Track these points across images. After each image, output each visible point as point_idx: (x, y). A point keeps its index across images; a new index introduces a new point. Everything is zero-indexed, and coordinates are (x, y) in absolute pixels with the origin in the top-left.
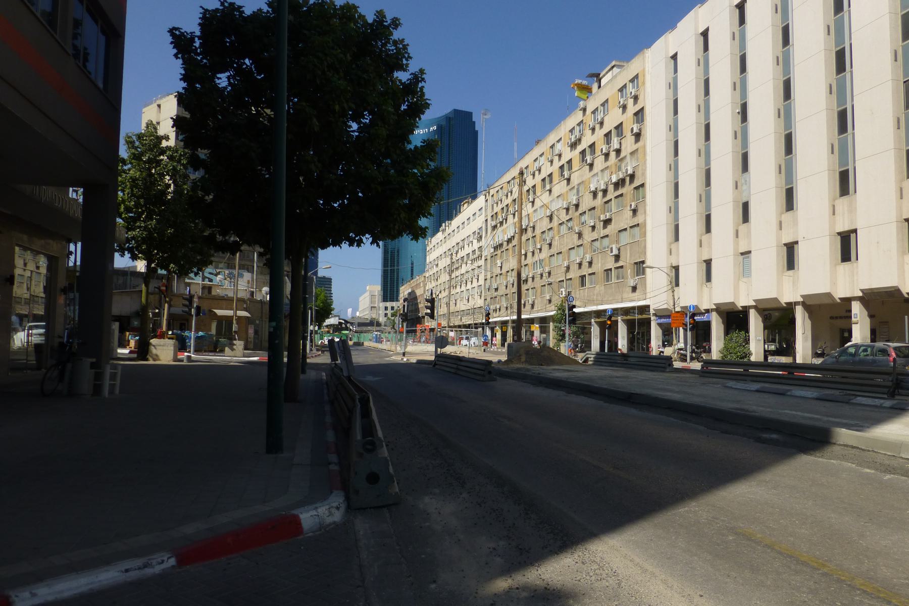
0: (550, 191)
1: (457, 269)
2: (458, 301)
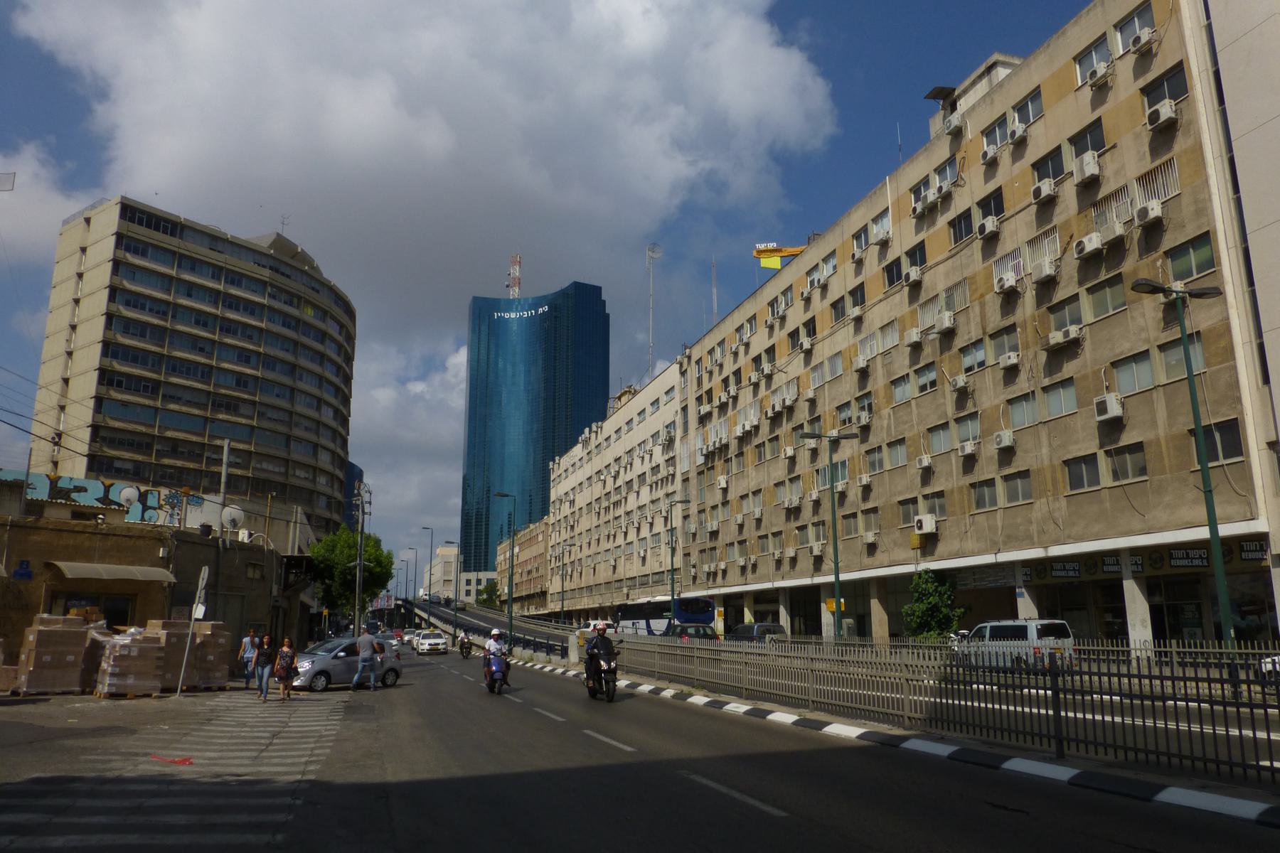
0: (859, 321)
1: (617, 504)
2: (621, 562)
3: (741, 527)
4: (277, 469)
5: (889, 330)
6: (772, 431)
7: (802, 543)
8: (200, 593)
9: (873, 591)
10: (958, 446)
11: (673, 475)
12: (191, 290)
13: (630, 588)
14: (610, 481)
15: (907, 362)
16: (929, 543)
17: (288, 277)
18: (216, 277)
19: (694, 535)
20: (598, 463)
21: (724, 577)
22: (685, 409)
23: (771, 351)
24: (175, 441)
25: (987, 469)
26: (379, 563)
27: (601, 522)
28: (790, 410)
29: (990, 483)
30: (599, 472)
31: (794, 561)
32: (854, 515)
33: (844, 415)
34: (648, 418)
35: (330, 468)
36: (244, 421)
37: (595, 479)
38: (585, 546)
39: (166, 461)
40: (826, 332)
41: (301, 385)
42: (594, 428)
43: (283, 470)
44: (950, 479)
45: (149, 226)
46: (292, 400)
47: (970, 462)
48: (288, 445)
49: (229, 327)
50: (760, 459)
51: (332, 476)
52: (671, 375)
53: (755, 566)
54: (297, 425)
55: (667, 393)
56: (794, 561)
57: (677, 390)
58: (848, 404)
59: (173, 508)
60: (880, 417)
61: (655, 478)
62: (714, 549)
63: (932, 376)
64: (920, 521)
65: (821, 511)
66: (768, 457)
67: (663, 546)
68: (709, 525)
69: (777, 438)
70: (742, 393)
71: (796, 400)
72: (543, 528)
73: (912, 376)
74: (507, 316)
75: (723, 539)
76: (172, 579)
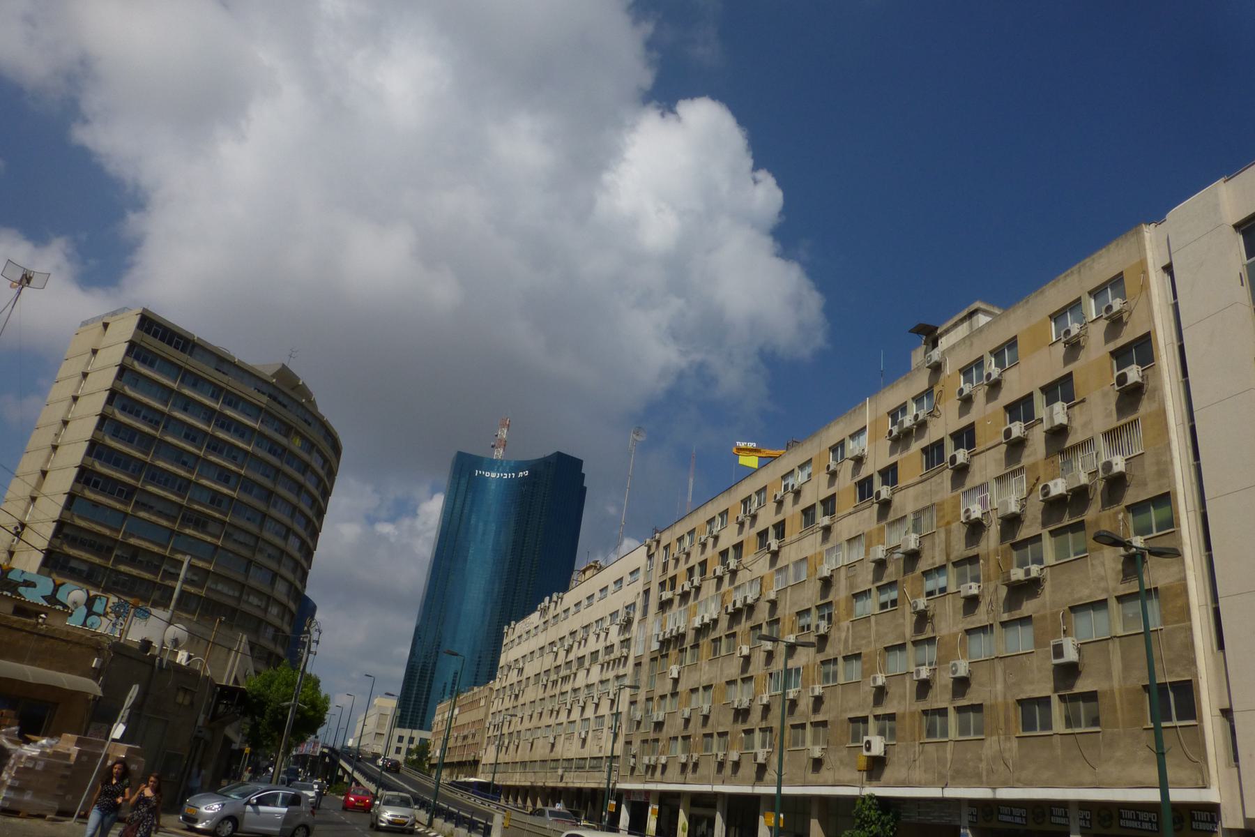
0: (827, 530)
3: (687, 721)
4: (231, 593)
5: (856, 544)
6: (730, 627)
7: (747, 748)
8: (124, 713)
9: (815, 809)
10: (913, 669)
11: (626, 658)
12: (188, 405)
13: (566, 769)
14: (562, 654)
15: (870, 577)
16: (876, 767)
17: (285, 406)
18: (215, 396)
19: (639, 723)
20: (553, 634)
21: (663, 772)
22: (647, 592)
23: (738, 547)
24: (137, 549)
25: (940, 698)
26: (314, 706)
27: (546, 695)
28: (751, 608)
29: (943, 712)
30: (552, 644)
31: (736, 765)
32: (803, 726)
33: (803, 622)
34: (609, 596)
35: (284, 599)
36: (209, 539)
37: (547, 650)
38: (526, 718)
39: (123, 568)
40: (795, 537)
41: (274, 512)
42: (555, 598)
43: (237, 594)
44: (902, 703)
45: (162, 339)
46: (261, 526)
47: (924, 687)
48: (247, 571)
49: (216, 446)
50: (715, 654)
51: (284, 607)
52: (639, 557)
53: (696, 765)
54: (261, 551)
55: (632, 573)
56: (736, 765)
57: (642, 572)
58: (808, 611)
59: (118, 618)
60: (839, 629)
61: (607, 658)
62: (657, 740)
63: (894, 594)
64: (868, 742)
65: (769, 717)
66: (723, 653)
67: (605, 730)
68: (655, 714)
69: (734, 635)
70: (705, 584)
71: (758, 600)
72: (487, 693)
73: (874, 591)
74: (487, 474)
75: (668, 731)
76: (99, 693)
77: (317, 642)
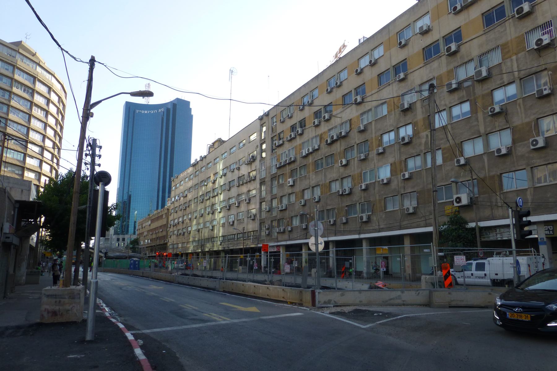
14: (210, 185)
43: (20, 173)
60: (419, 138)
74: (143, 112)
77: (100, 156)
